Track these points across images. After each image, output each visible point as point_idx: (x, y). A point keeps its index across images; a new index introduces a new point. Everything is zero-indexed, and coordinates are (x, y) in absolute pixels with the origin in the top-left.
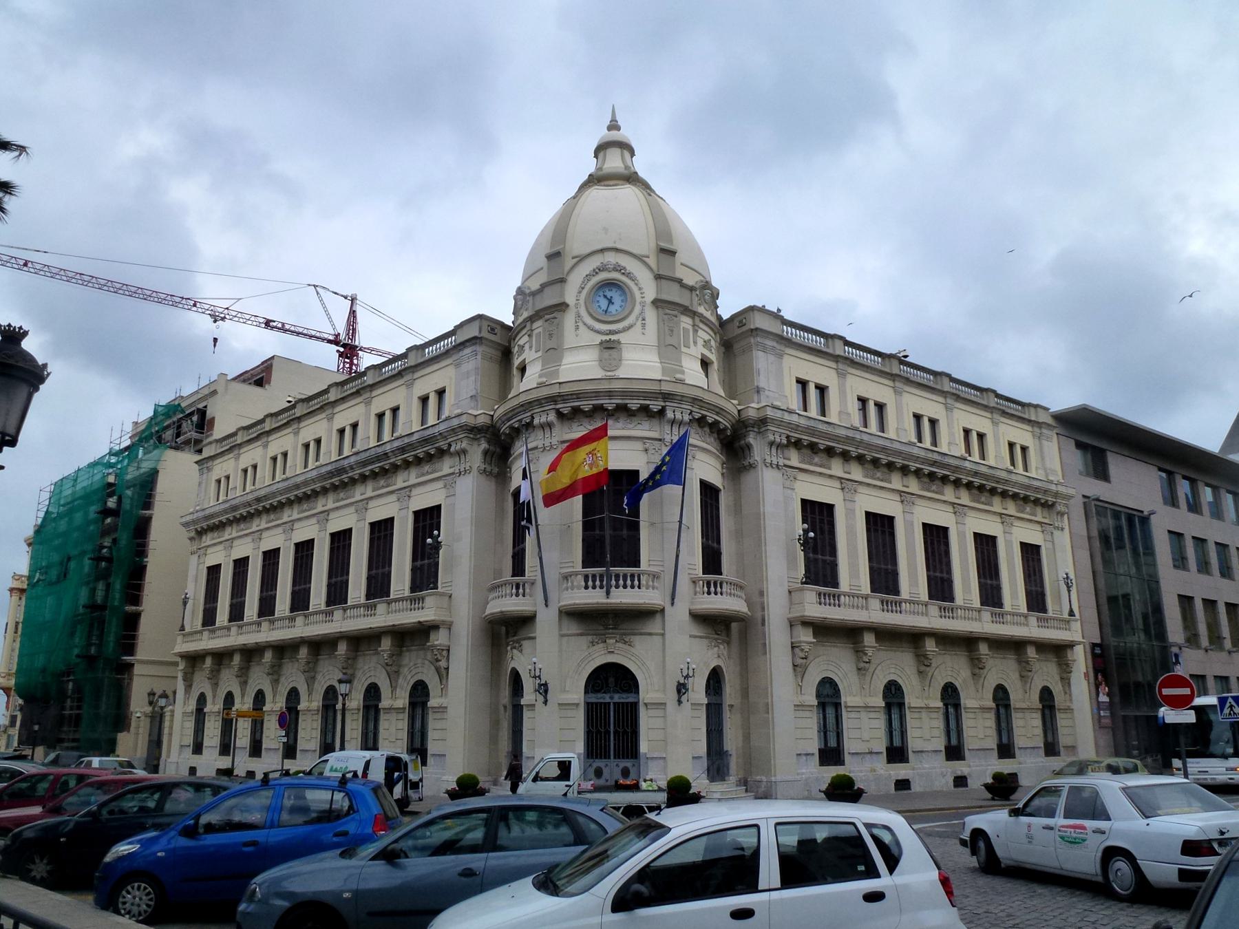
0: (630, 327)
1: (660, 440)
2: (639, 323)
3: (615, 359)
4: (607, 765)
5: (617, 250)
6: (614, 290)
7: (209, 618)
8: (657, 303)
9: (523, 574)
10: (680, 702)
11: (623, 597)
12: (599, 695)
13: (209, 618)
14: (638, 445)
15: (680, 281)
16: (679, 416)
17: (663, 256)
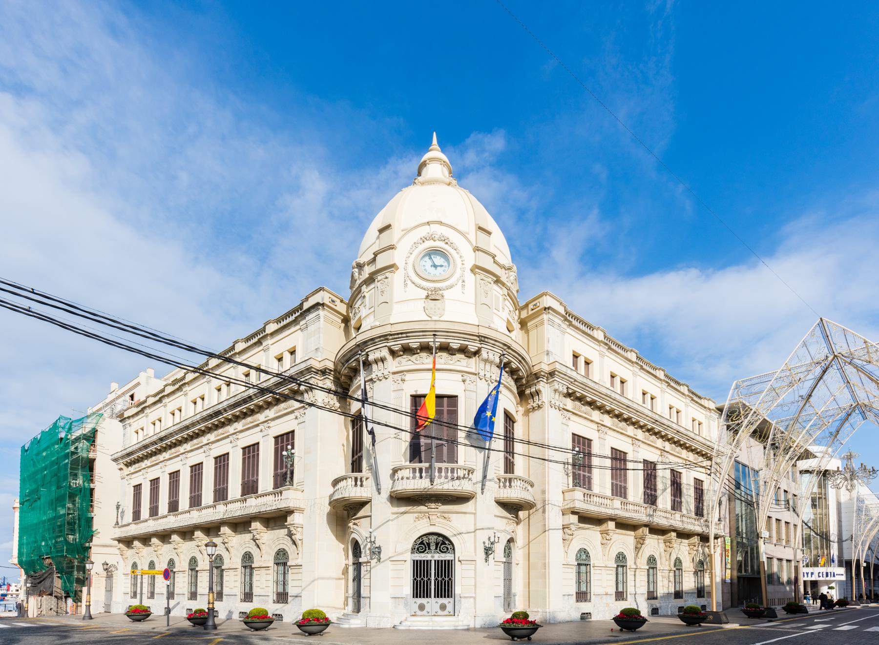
0: (451, 287)
1: (476, 374)
2: (460, 283)
3: (439, 309)
4: (428, 602)
5: (441, 223)
6: (438, 257)
7: (137, 515)
8: (476, 269)
9: (360, 471)
10: (486, 560)
11: (443, 485)
12: (423, 555)
13: (137, 515)
14: (458, 376)
15: (494, 257)
16: (491, 357)
17: (480, 233)
